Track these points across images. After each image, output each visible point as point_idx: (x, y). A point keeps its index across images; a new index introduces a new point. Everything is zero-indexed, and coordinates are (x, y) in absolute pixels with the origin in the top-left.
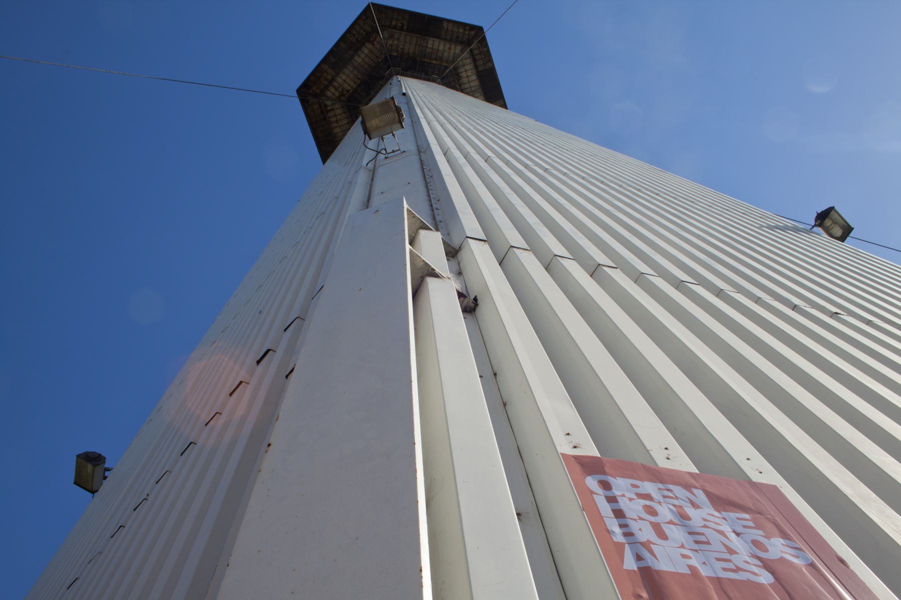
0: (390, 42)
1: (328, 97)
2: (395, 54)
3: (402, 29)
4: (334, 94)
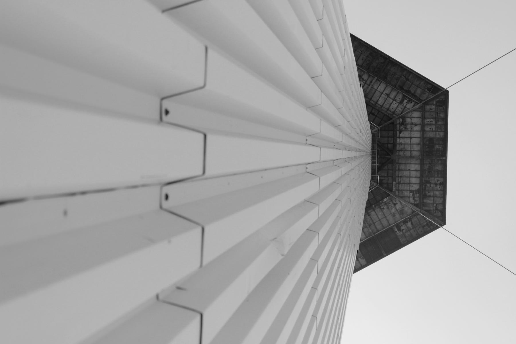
0: (398, 206)
1: (414, 111)
2: (385, 200)
3: (398, 226)
4: (411, 118)
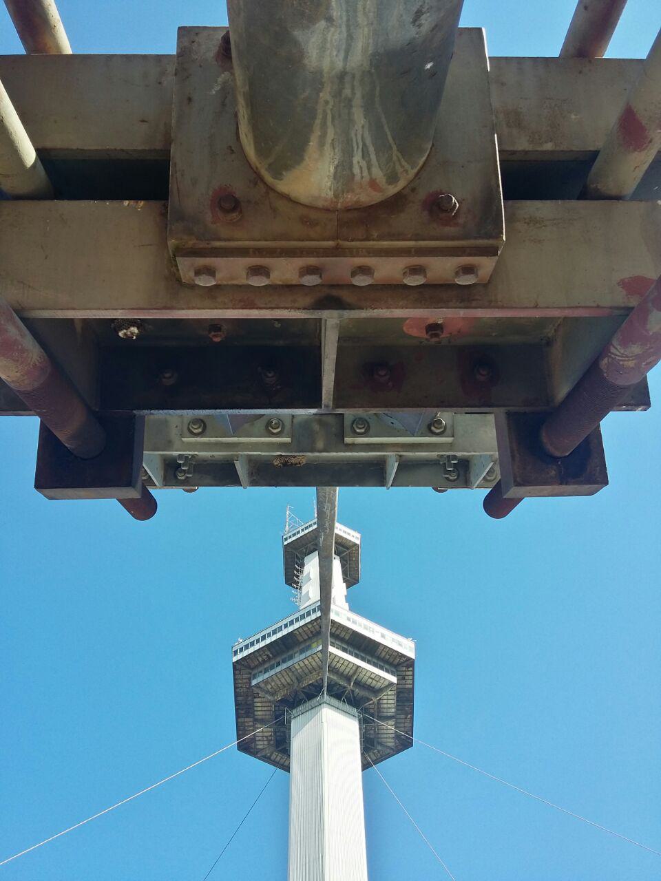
0: (269, 687)
3: (269, 658)
